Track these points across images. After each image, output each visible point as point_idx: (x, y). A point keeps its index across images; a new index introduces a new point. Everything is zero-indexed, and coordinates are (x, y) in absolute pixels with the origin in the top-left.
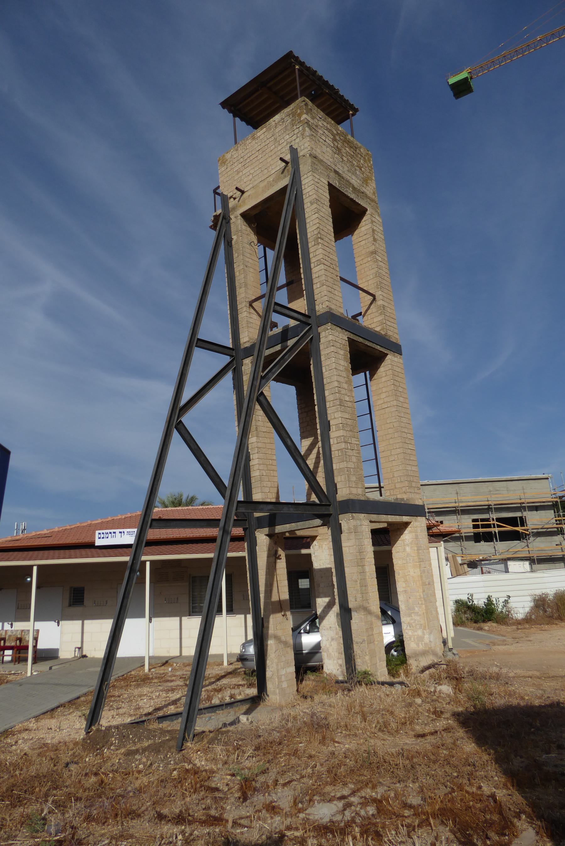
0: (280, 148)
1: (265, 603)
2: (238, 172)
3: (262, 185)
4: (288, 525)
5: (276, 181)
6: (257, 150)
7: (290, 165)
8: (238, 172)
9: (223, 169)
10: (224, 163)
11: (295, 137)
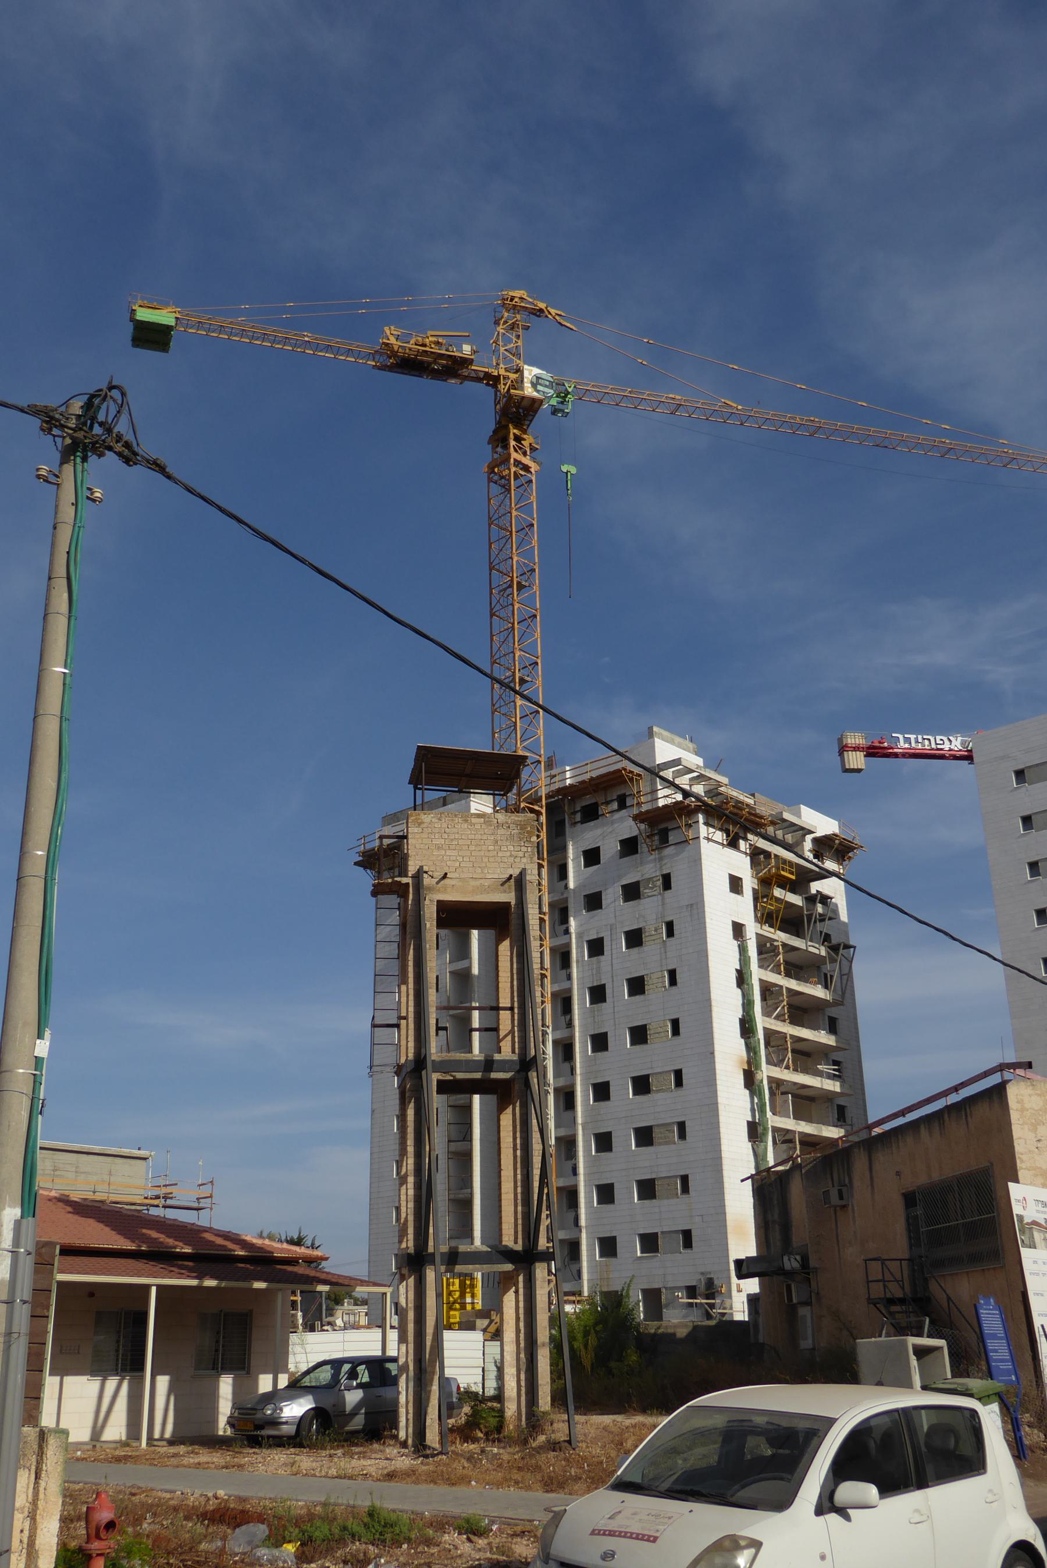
0: (500, 854)
1: (432, 1347)
2: (439, 848)
3: (473, 883)
4: (471, 1266)
5: (490, 889)
6: (470, 837)
7: (513, 880)
8: (439, 848)
9: (416, 830)
10: (420, 824)
11: (521, 854)
